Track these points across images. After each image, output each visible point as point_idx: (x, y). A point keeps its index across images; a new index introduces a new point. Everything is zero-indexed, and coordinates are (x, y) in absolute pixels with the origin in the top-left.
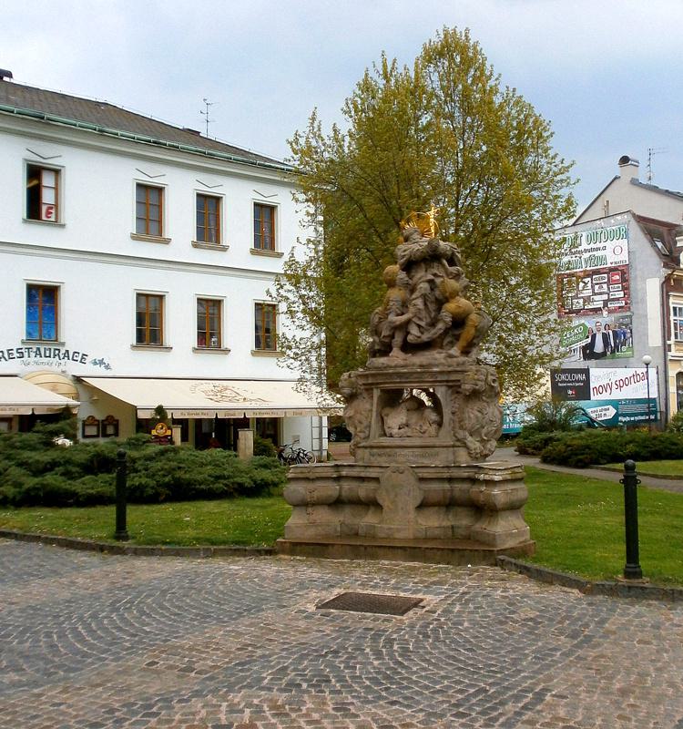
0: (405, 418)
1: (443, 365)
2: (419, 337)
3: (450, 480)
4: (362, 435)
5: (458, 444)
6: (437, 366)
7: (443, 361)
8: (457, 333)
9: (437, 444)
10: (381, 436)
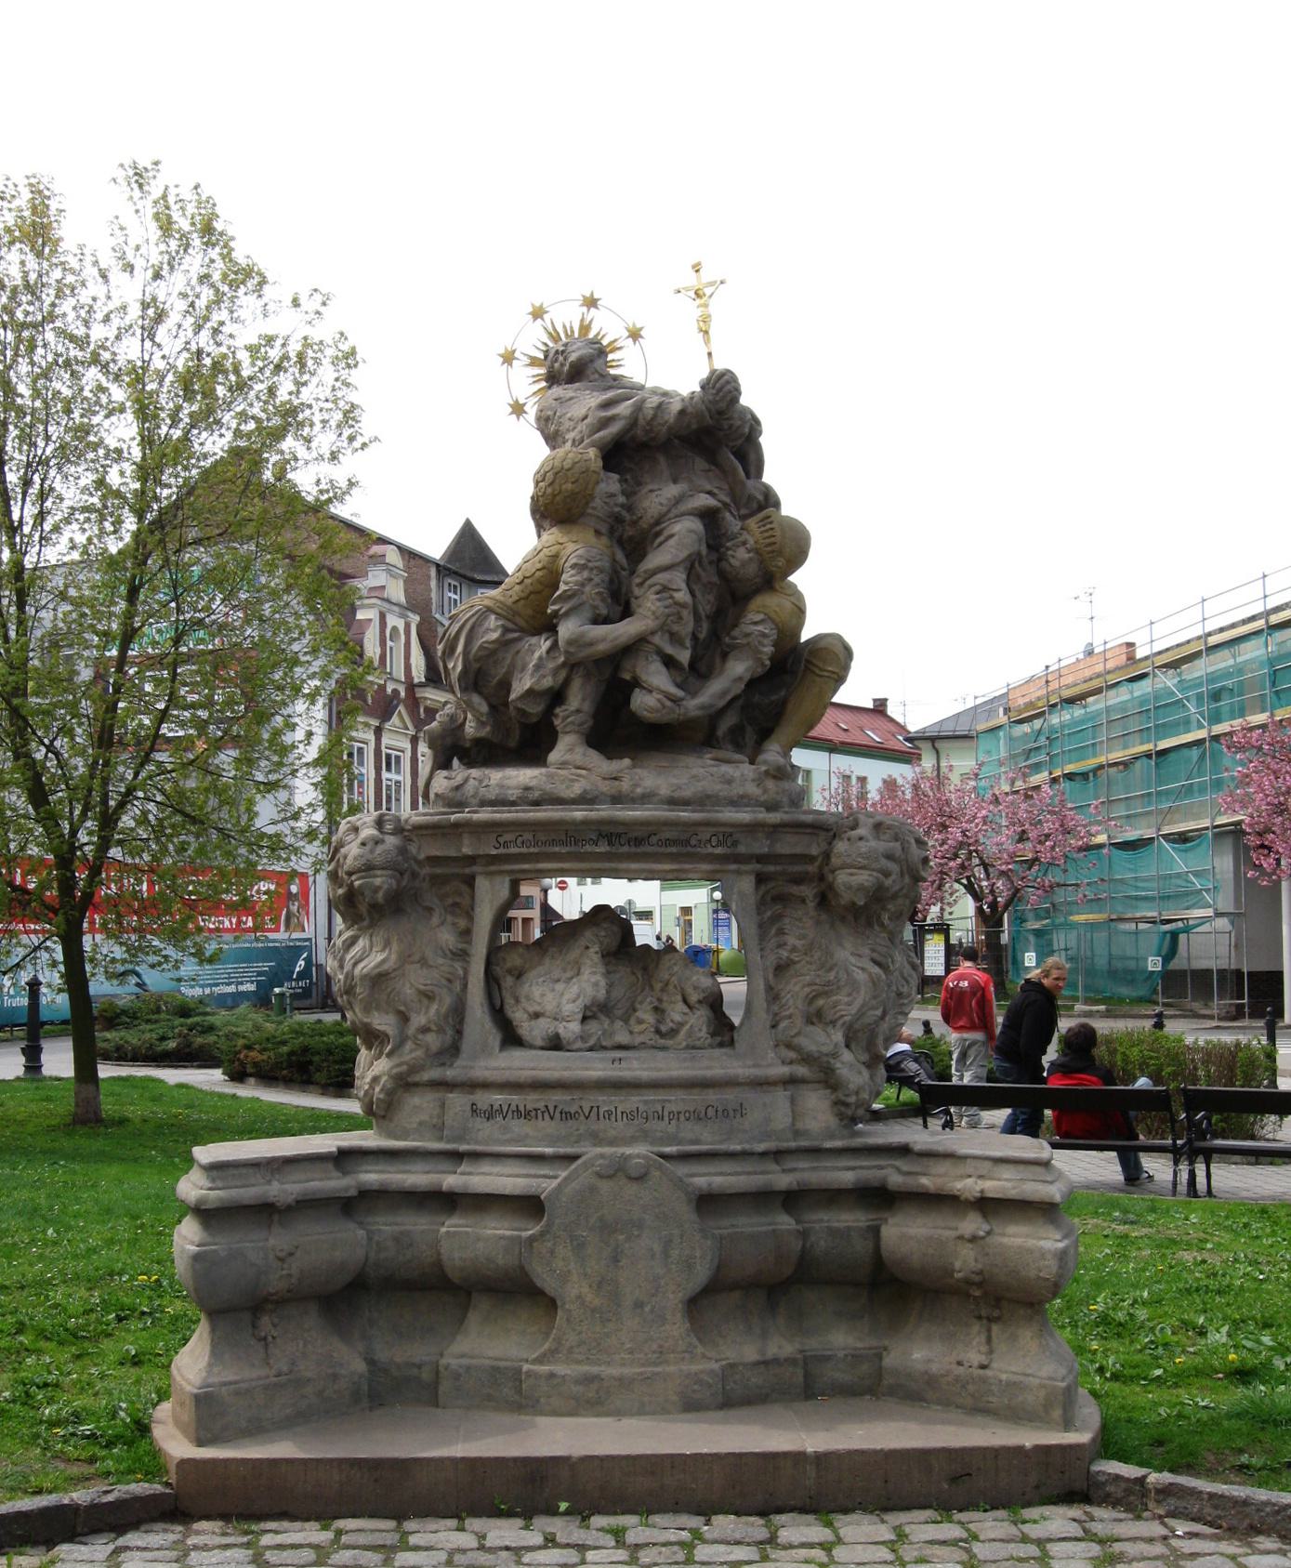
0: (603, 983)
2: (675, 701)
3: (792, 1200)
5: (802, 1071)
7: (752, 789)
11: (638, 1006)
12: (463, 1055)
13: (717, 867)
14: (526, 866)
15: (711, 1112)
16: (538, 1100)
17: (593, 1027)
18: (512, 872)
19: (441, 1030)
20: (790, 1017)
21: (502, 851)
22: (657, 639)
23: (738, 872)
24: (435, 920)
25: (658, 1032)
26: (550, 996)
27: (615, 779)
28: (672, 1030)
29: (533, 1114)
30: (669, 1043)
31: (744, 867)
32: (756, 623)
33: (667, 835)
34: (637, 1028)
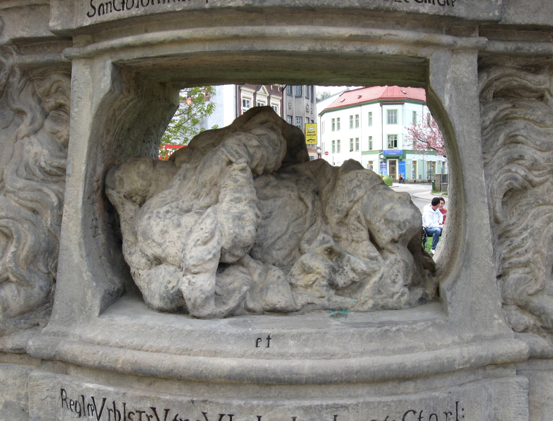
0: (250, 215)
11: (305, 246)
12: (56, 317)
13: (422, 36)
14: (129, 40)
16: (142, 398)
18: (113, 50)
19: (22, 282)
20: (526, 264)
21: (97, 19)
23: (453, 49)
24: (24, 127)
25: (332, 285)
26: (174, 233)
28: (353, 282)
30: (347, 301)
31: (462, 42)
34: (303, 280)
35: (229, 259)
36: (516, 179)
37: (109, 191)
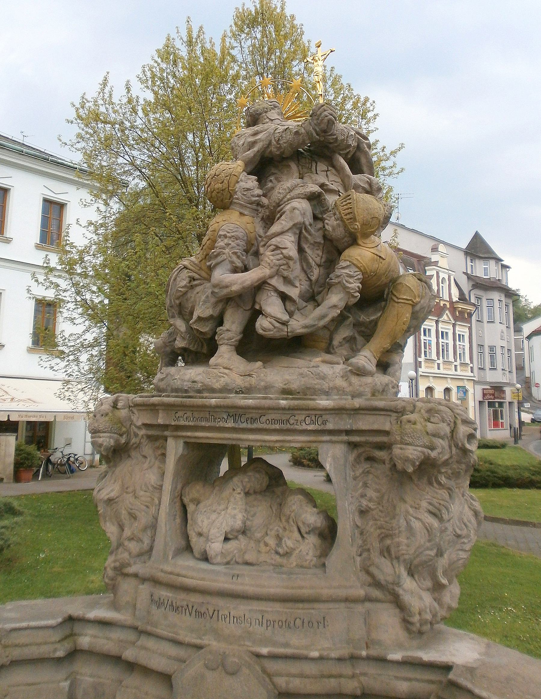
0: (240, 516)
1: (340, 391)
2: (285, 323)
4: (133, 546)
5: (376, 593)
6: (327, 393)
7: (340, 382)
8: (363, 318)
9: (326, 592)
10: (178, 552)
11: (269, 532)
12: (152, 559)
13: (312, 438)
14: (189, 434)
15: (298, 622)
16: (183, 600)
17: (232, 545)
22: (274, 282)
27: (249, 375)
28: (287, 553)
29: (180, 609)
30: (284, 561)
32: (343, 268)
33: (270, 417)
35: (230, 536)
36: (362, 507)
37: (183, 498)
